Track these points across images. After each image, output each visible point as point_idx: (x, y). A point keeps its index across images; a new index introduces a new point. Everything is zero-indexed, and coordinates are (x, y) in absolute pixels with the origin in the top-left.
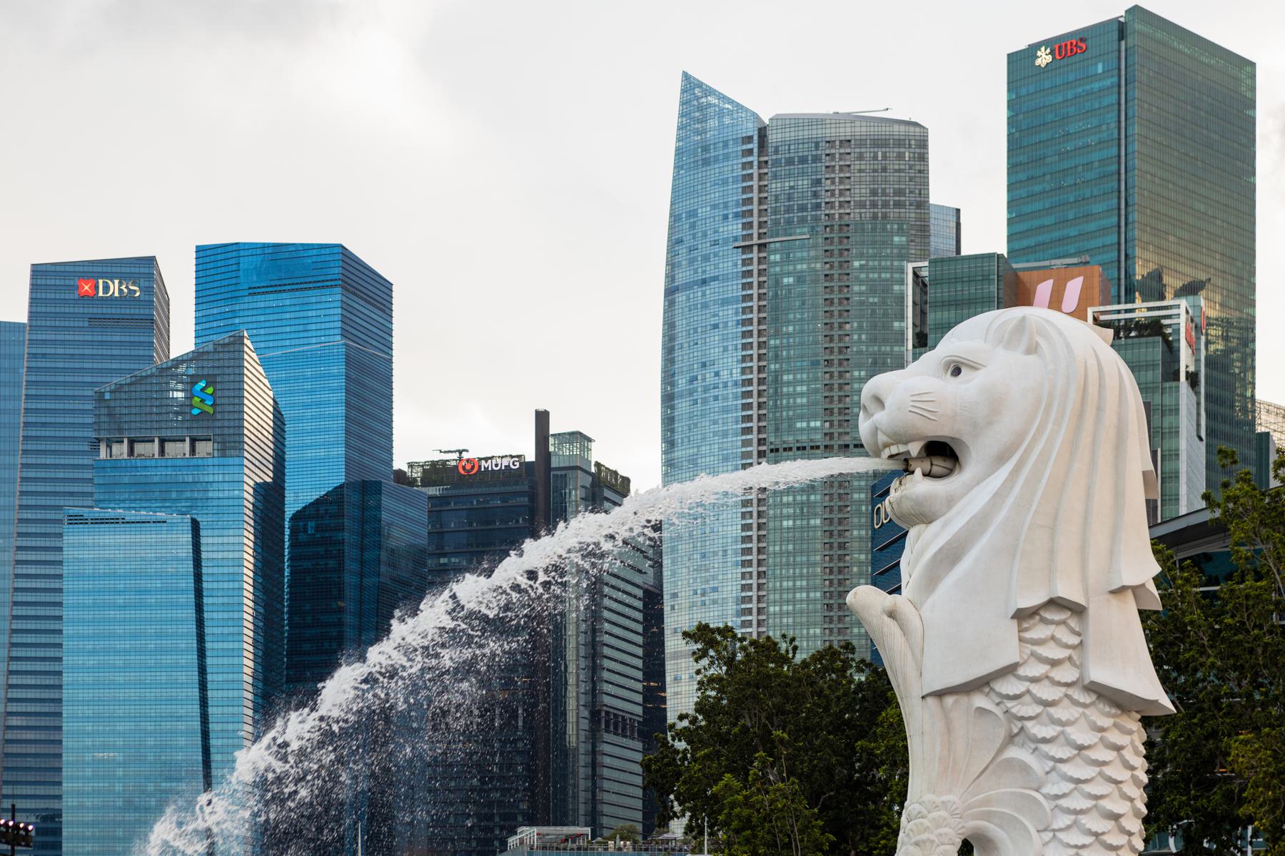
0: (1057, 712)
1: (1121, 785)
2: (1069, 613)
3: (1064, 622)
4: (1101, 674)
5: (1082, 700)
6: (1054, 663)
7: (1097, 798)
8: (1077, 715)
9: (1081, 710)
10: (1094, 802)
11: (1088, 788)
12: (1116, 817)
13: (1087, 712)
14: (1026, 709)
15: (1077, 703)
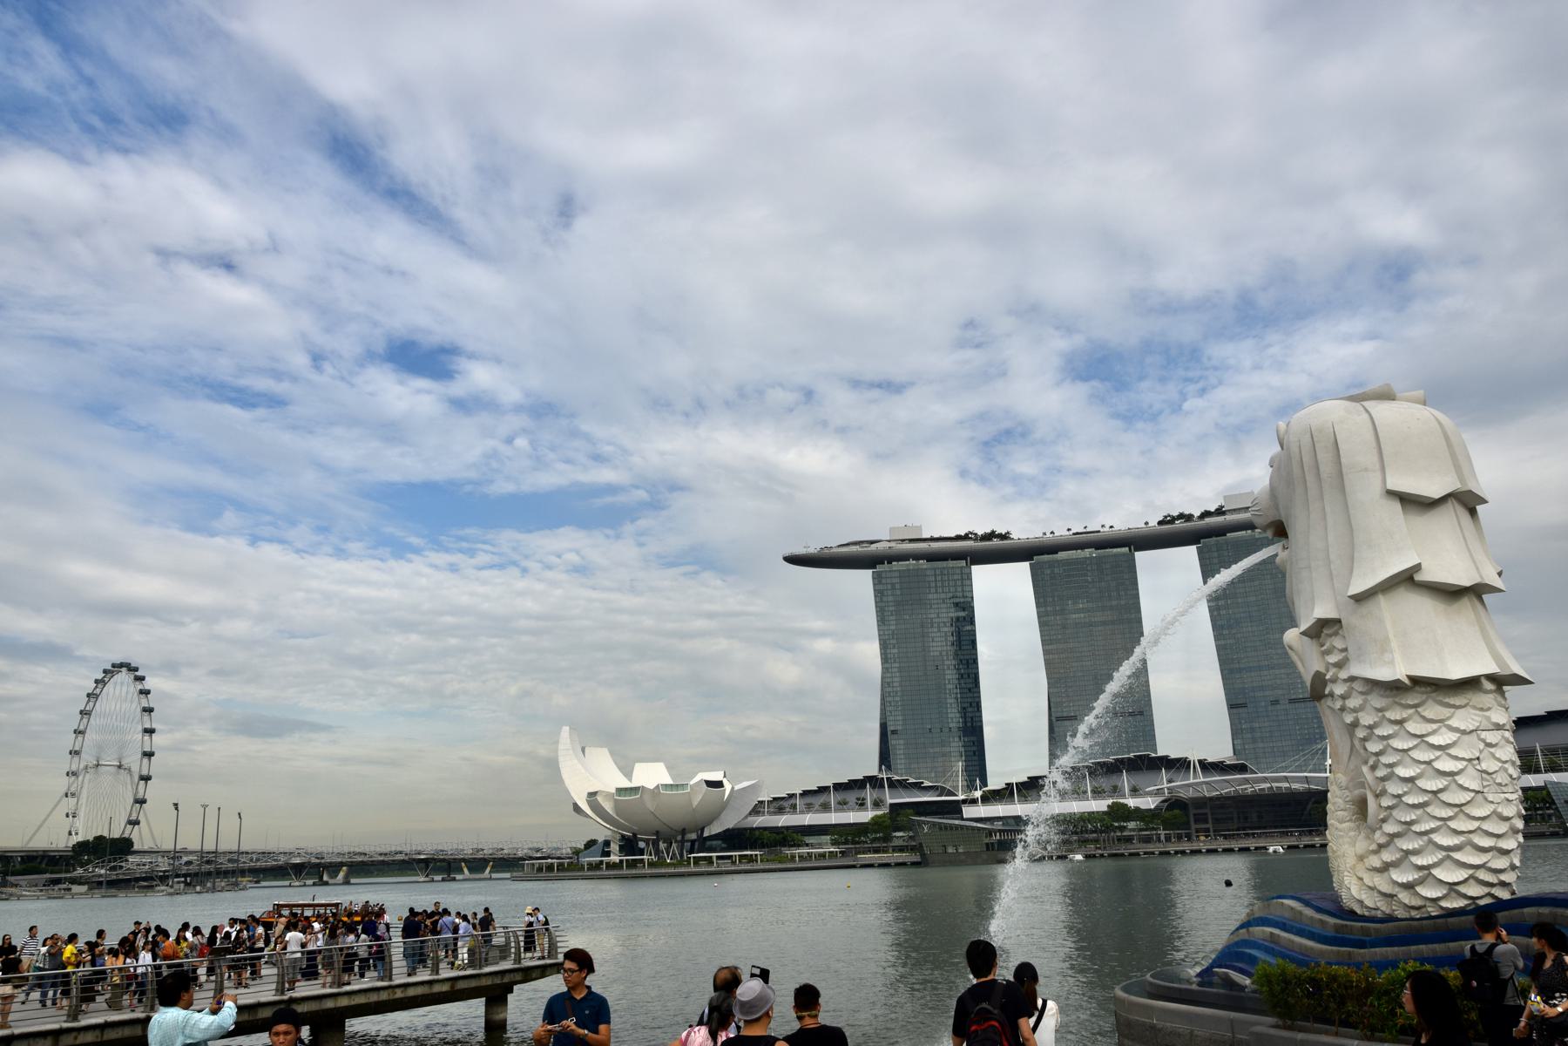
0: (1353, 703)
1: (1410, 753)
2: (1339, 624)
3: (1336, 634)
4: (1356, 669)
5: (1360, 690)
6: (1339, 665)
7: (1391, 766)
8: (1361, 702)
9: (1363, 697)
10: (1389, 770)
11: (1385, 760)
12: (1411, 780)
13: (1369, 697)
14: (1338, 704)
15: (1362, 693)
